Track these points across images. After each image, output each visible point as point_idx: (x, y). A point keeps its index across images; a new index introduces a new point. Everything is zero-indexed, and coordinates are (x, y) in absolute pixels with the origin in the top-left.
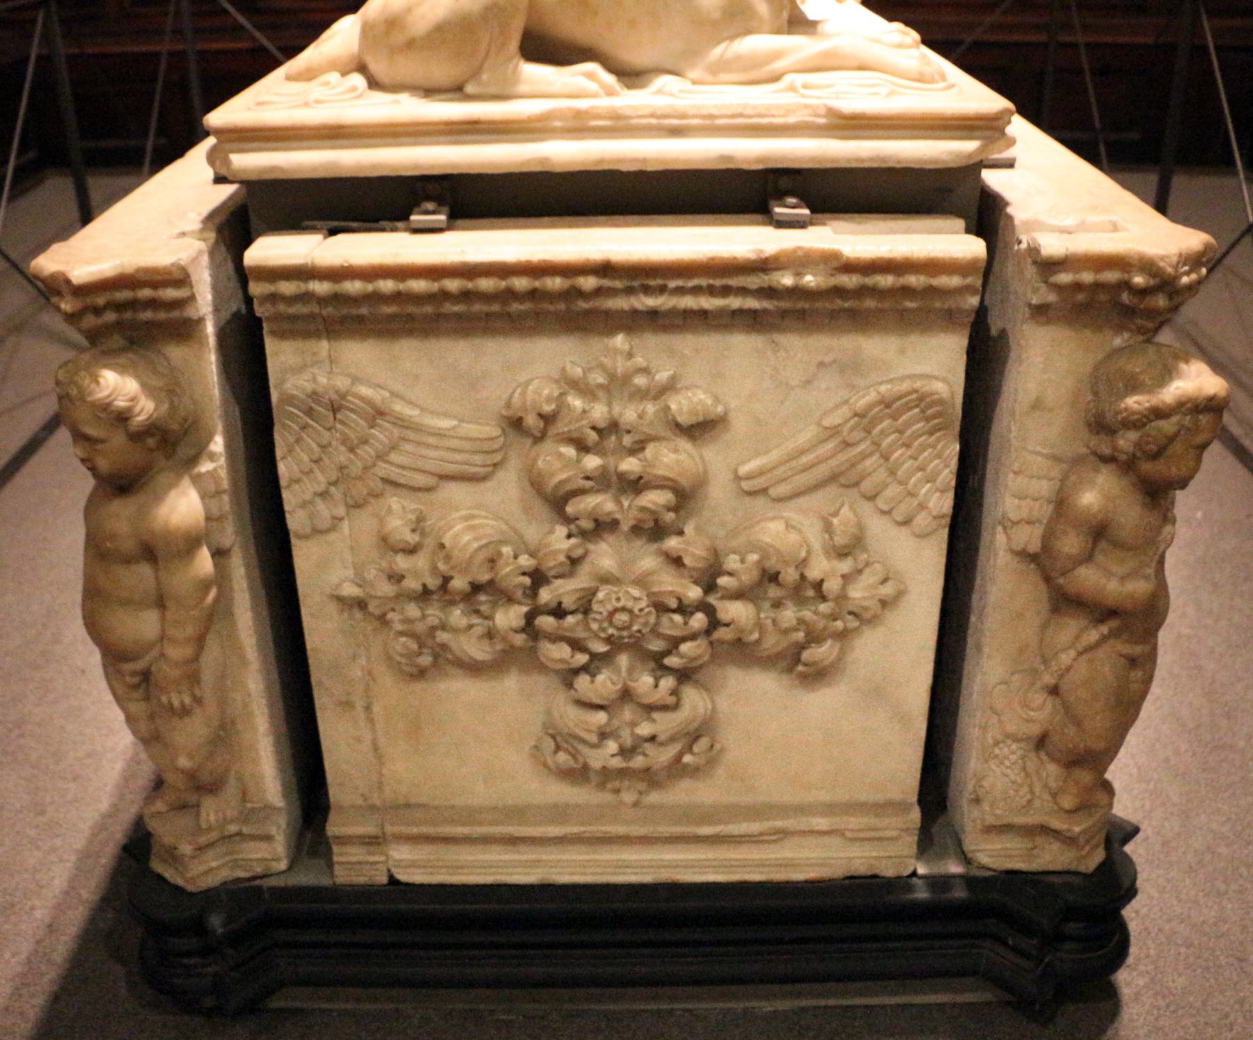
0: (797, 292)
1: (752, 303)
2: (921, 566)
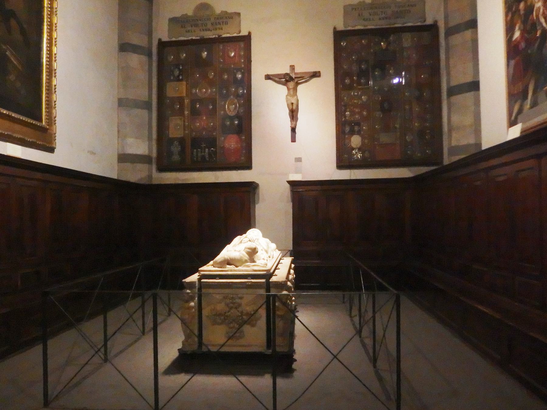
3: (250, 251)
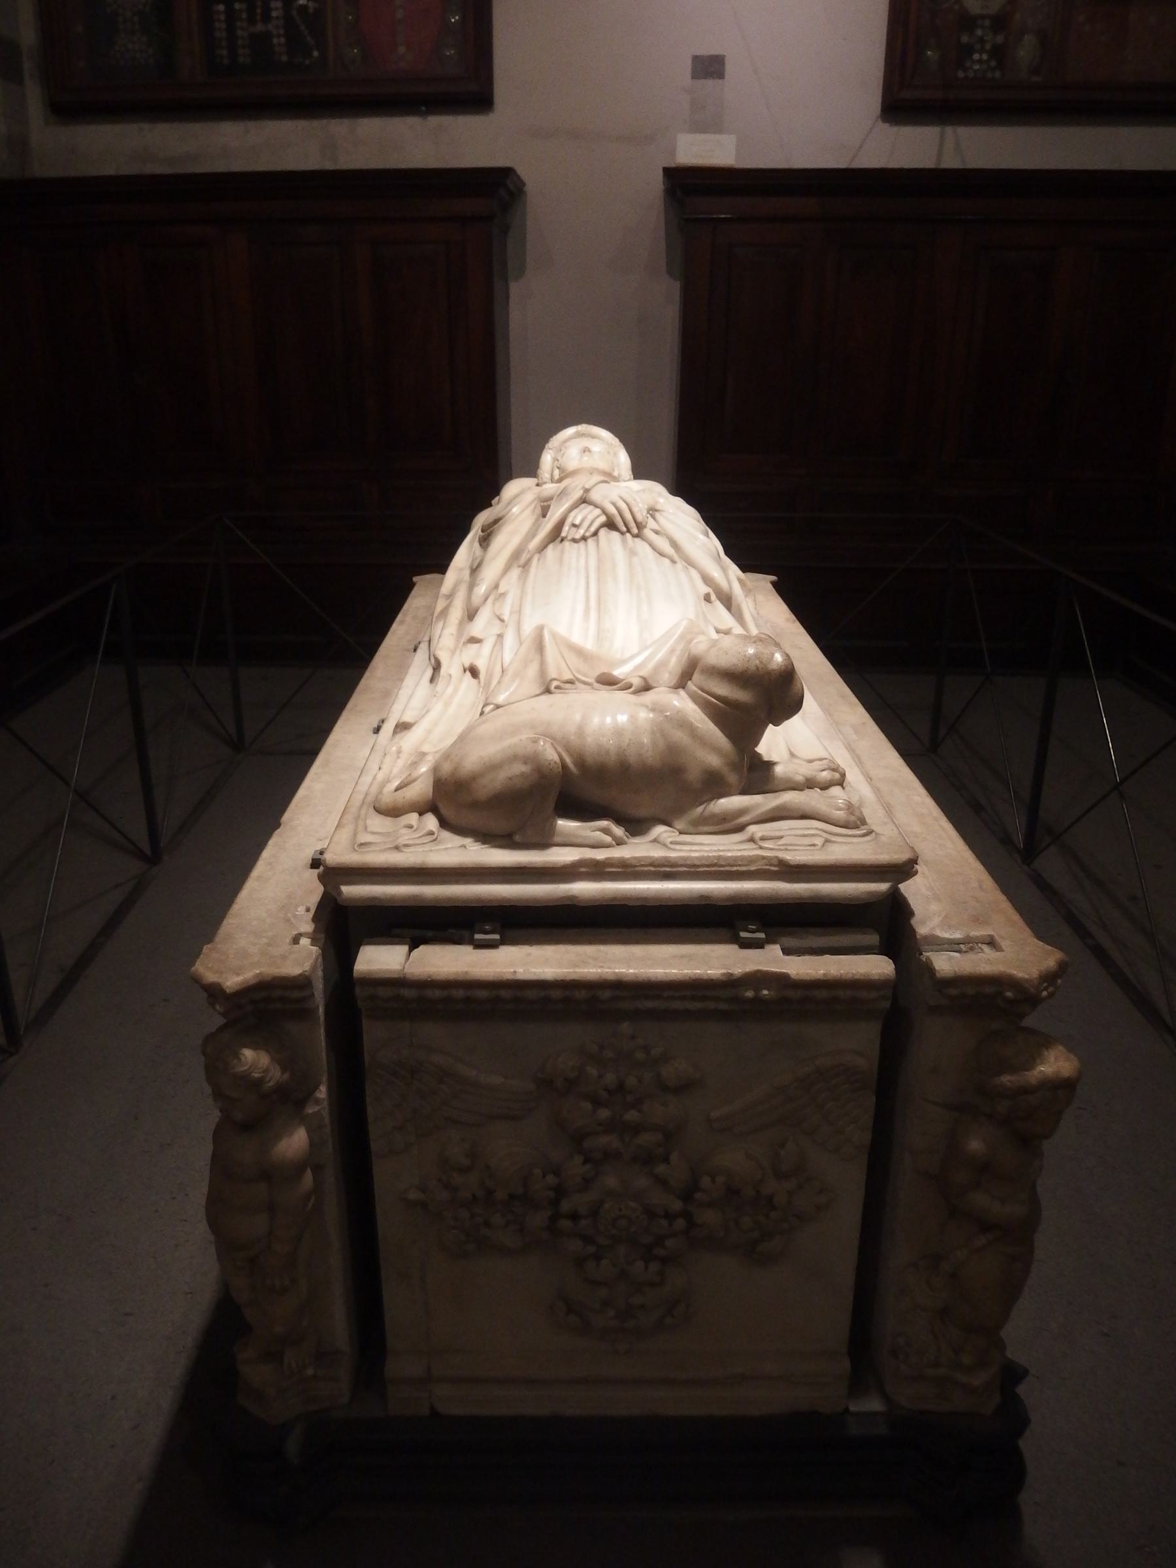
0: (757, 1000)
1: (723, 1006)
2: (847, 1181)
3: (741, 695)
